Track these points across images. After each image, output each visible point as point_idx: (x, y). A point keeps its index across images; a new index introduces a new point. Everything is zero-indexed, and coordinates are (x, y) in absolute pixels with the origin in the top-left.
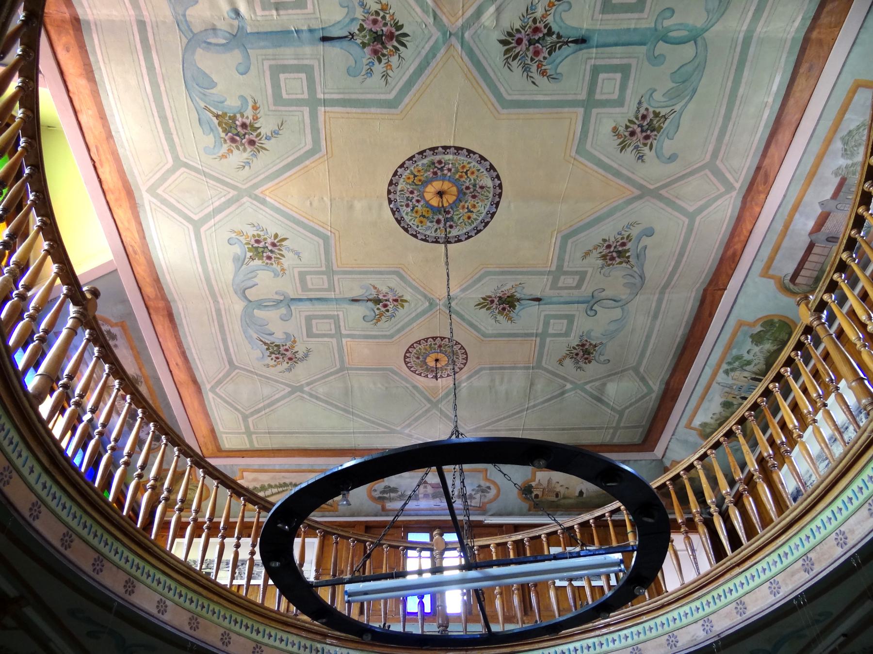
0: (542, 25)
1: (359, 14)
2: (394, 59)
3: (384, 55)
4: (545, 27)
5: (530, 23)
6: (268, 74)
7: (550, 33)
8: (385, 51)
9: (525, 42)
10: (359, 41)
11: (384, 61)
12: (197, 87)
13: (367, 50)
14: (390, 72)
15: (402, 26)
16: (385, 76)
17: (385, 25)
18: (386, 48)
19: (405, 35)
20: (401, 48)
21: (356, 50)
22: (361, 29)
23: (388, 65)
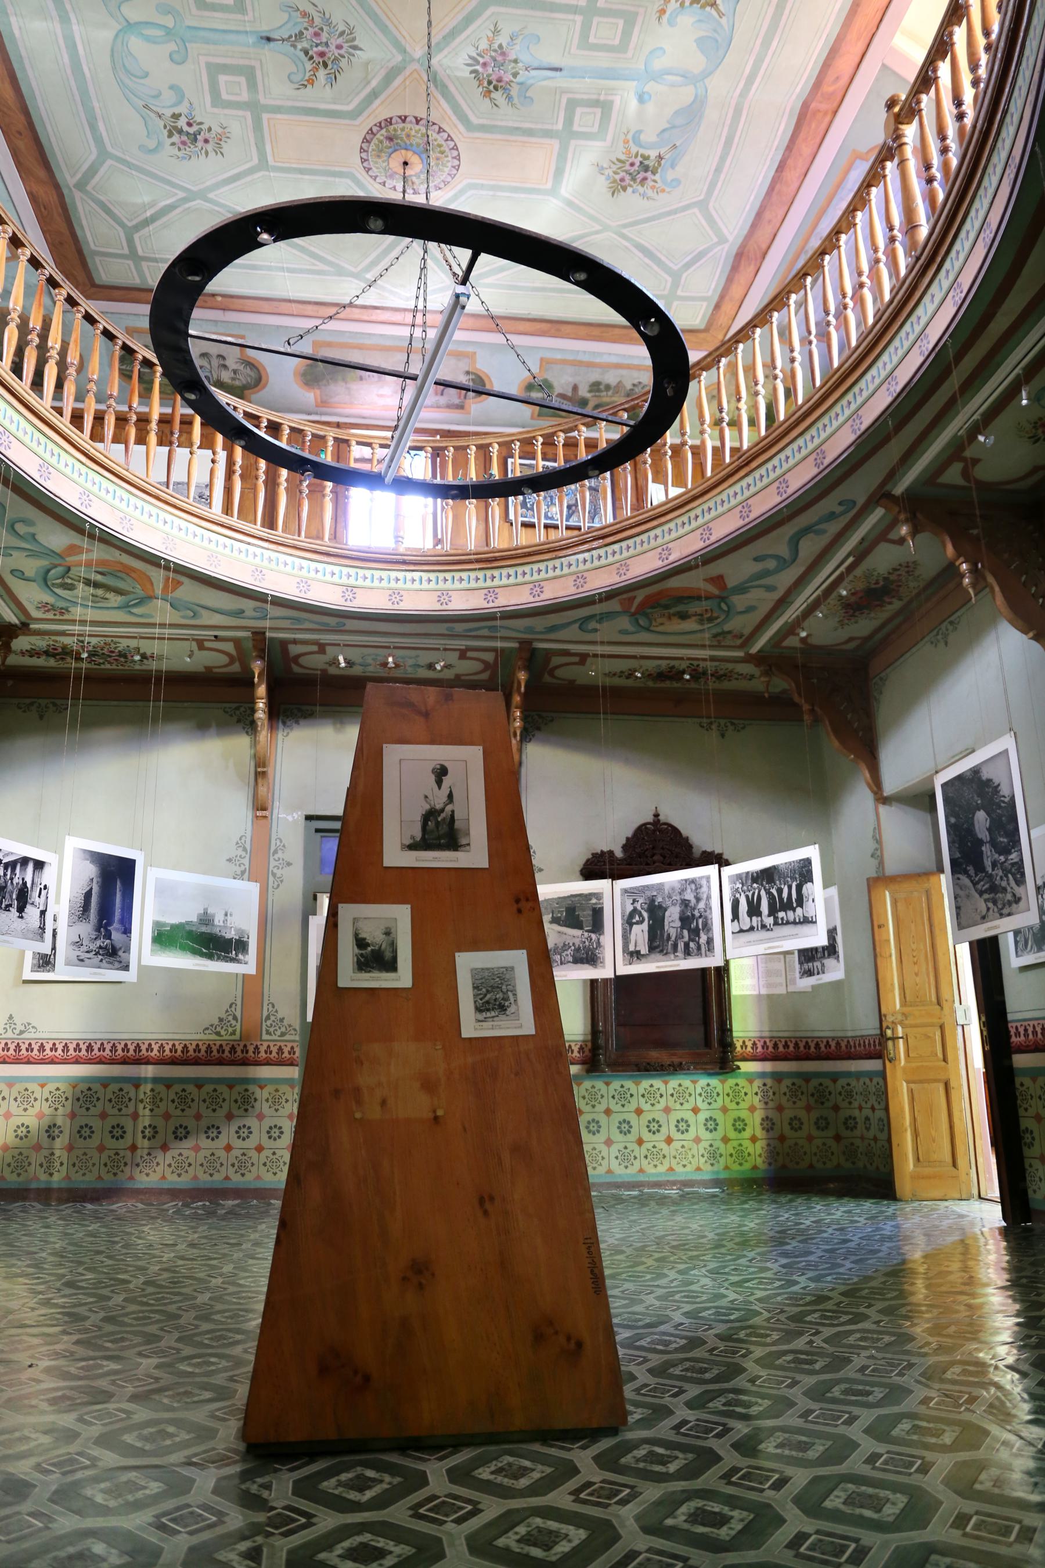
0: (316, 58)
1: (514, 91)
2: (484, 45)
3: (495, 51)
4: (311, 58)
5: (329, 63)
6: (632, 45)
7: (306, 53)
8: (493, 54)
9: (333, 47)
10: (520, 65)
11: (496, 46)
12: (720, 40)
13: (512, 56)
14: (490, 35)
15: (472, 72)
16: (496, 31)
17: (489, 75)
18: (491, 57)
19: (468, 65)
20: (475, 55)
21: (525, 58)
22: (515, 75)
23: (491, 42)
